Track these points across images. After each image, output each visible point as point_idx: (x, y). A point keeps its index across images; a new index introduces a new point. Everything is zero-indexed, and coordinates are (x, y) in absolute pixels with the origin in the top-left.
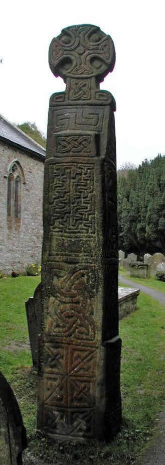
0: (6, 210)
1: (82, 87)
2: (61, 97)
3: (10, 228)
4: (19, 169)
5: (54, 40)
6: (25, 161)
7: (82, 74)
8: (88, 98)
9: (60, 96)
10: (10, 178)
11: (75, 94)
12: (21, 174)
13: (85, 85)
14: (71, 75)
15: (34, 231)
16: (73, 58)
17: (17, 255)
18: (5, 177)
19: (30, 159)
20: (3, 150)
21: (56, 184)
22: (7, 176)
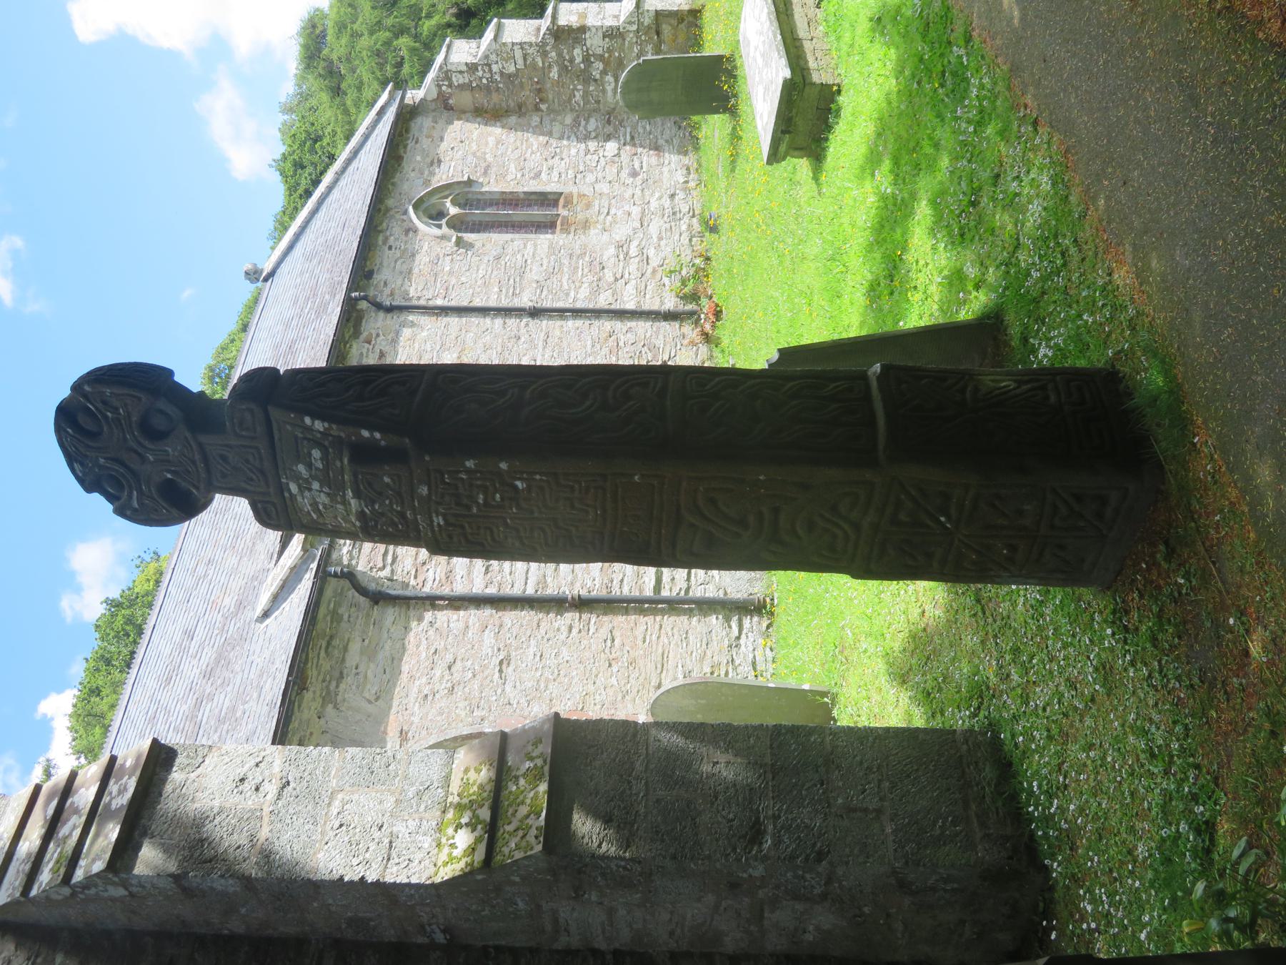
0: (542, 236)
2: (265, 510)
3: (586, 225)
4: (434, 200)
5: (120, 511)
6: (413, 185)
7: (194, 462)
10: (458, 224)
11: (252, 480)
12: (447, 193)
13: (224, 458)
14: (202, 486)
15: (592, 150)
17: (654, 204)
18: (459, 242)
19: (404, 164)
20: (390, 248)
22: (454, 239)
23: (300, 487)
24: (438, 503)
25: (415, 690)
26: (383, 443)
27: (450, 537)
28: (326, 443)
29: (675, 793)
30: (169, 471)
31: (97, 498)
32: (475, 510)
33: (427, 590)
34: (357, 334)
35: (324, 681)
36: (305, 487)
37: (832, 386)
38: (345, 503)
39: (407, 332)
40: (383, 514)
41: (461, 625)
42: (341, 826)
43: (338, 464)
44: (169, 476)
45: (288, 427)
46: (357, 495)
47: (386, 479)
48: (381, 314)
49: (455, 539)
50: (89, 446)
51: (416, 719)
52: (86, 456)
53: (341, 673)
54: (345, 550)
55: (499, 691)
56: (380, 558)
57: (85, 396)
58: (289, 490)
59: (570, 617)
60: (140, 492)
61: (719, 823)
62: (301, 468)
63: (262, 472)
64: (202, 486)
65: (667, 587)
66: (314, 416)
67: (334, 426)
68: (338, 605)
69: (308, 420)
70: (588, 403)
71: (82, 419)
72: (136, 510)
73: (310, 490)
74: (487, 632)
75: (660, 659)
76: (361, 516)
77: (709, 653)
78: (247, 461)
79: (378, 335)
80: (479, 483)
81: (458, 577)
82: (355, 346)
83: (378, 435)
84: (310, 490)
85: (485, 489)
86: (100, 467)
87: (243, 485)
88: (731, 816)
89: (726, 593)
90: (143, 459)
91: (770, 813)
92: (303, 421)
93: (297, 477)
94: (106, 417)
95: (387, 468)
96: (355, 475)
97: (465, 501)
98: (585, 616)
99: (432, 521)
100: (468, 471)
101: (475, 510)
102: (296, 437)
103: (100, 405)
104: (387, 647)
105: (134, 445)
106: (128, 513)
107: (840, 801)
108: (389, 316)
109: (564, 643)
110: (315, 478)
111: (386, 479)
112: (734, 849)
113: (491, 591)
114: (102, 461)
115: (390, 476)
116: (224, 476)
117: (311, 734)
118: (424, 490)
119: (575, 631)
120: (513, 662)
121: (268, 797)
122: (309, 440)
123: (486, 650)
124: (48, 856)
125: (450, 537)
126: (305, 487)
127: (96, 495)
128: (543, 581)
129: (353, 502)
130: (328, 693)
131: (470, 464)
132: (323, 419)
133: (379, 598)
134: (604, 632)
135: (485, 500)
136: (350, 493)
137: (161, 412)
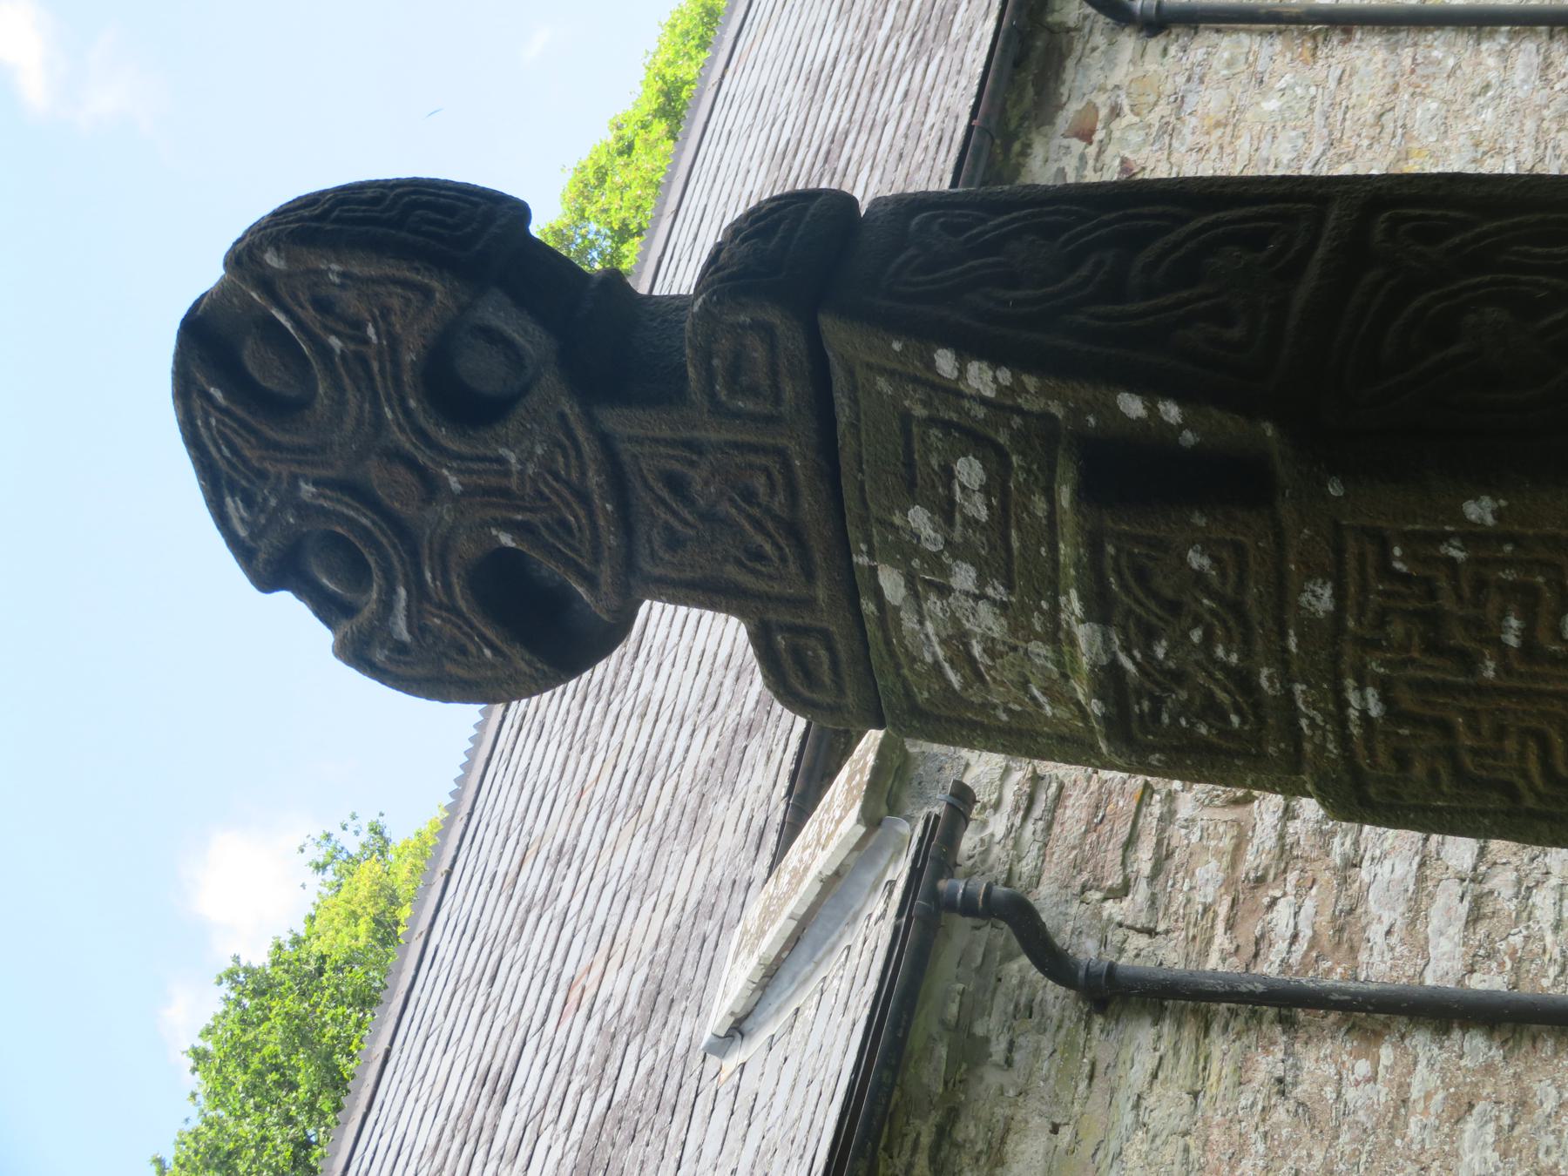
1: (688, 501)
2: (797, 653)
7: (584, 498)
8: (775, 470)
9: (787, 662)
11: (760, 556)
13: (676, 484)
14: (605, 573)
16: (466, 549)
21: (1525, 775)
23: (911, 580)
24: (1367, 644)
26: (1188, 438)
27: (1402, 759)
28: (1003, 438)
30: (508, 525)
31: (288, 606)
32: (1489, 671)
33: (1269, 968)
34: (1044, 106)
36: (928, 581)
38: (1057, 636)
39: (1210, 101)
40: (1178, 677)
41: (1382, 1094)
43: (1040, 506)
44: (506, 540)
45: (882, 384)
46: (1099, 609)
47: (1197, 560)
48: (1129, 42)
49: (1419, 769)
50: (277, 446)
52: (262, 475)
54: (998, 825)
56: (1113, 855)
57: (266, 284)
58: (878, 594)
60: (419, 592)
62: (919, 518)
63: (794, 531)
64: (605, 573)
66: (967, 349)
67: (1031, 382)
68: (974, 1006)
69: (945, 362)
71: (254, 358)
72: (401, 648)
73: (944, 591)
74: (1470, 1125)
76: (1109, 679)
78: (749, 496)
79: (1116, 112)
80: (1509, 575)
81: (1376, 932)
82: (1038, 150)
83: (1171, 412)
84: (944, 591)
85: (1526, 600)
86: (303, 509)
87: (732, 572)
90: (431, 487)
92: (930, 365)
93: (904, 551)
94: (325, 352)
95: (1199, 520)
96: (1094, 543)
97: (1458, 637)
99: (1343, 704)
100: (1473, 536)
101: (1489, 671)
102: (906, 417)
103: (309, 315)
105: (405, 442)
106: (379, 656)
108: (1155, 45)
110: (959, 551)
111: (1197, 560)
113: (1490, 982)
114: (307, 490)
115: (1207, 547)
116: (674, 542)
118: (1320, 599)
122: (947, 426)
125: (1402, 759)
126: (928, 581)
127: (285, 601)
129: (1082, 632)
131: (1480, 510)
132: (995, 360)
133: (1114, 995)
135: (1527, 635)
136: (1073, 603)
137: (491, 335)
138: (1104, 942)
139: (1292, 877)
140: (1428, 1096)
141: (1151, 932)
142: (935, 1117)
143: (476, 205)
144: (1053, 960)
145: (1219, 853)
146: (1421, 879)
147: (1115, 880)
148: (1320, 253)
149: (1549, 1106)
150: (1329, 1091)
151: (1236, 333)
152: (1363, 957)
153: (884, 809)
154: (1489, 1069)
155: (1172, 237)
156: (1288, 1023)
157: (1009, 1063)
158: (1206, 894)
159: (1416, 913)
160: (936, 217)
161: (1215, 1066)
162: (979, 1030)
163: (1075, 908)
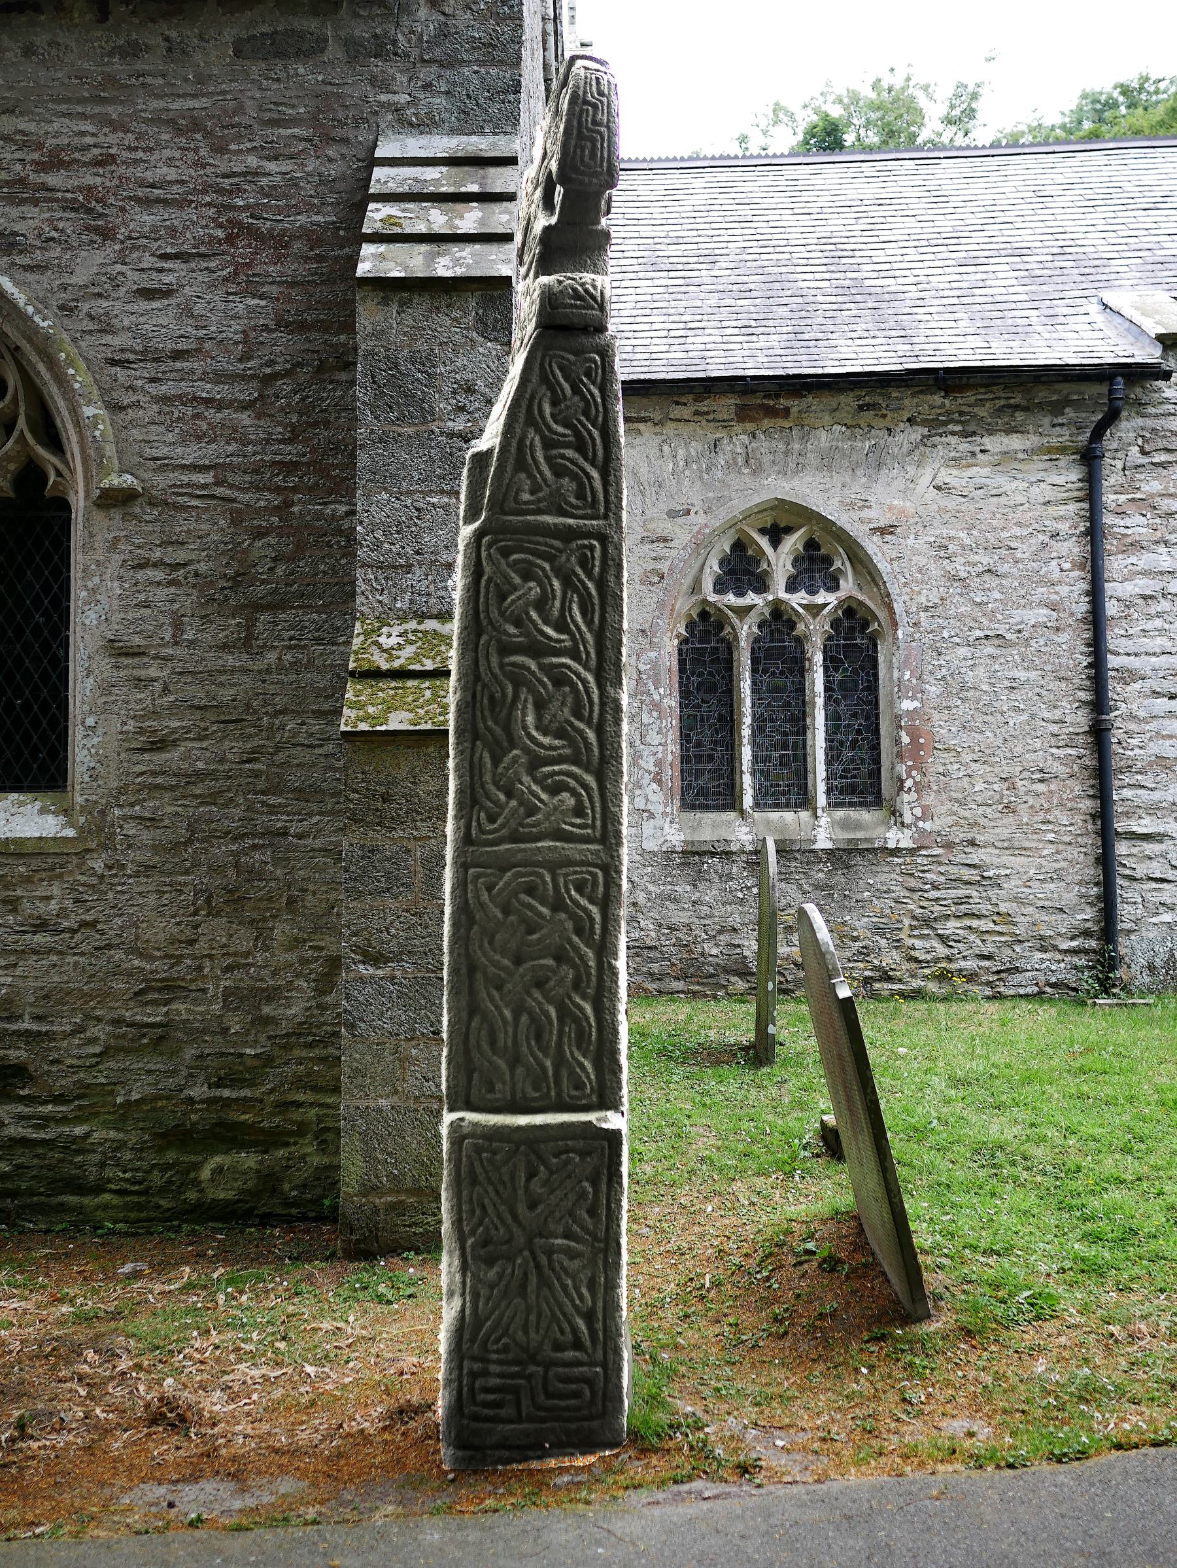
25: (953, 533)
29: (419, 869)
33: (1108, 519)
35: (961, 413)
37: (587, 1064)
41: (1056, 575)
42: (418, 509)
51: (911, 541)
53: (974, 434)
55: (957, 640)
59: (1081, 720)
61: (385, 918)
65: (1135, 851)
68: (1078, 405)
70: (546, 741)
74: (1046, 611)
75: (1016, 844)
77: (1030, 910)
81: (1133, 559)
88: (393, 931)
89: (1130, 932)
91: (398, 974)
98: (1080, 740)
104: (1015, 484)
107: (414, 1052)
109: (1033, 716)
112: (355, 934)
113: (1111, 608)
117: (884, 416)
119: (1055, 728)
120: (1003, 651)
121: (450, 424)
123: (1018, 615)
124: (411, 206)
128: (1131, 676)
130: (945, 423)
133: (1090, 459)
134: (1057, 768)
138: (1116, 450)
139: (1158, 521)
140: (1057, 593)
141: (1124, 469)
142: (1024, 403)
143: (601, 166)
144: (1098, 433)
145: (1166, 488)
146: (1161, 573)
147: (1147, 448)
148: (571, 521)
149: (1058, 640)
150: (1054, 555)
151: (526, 497)
152: (1120, 556)
153: (1169, 343)
154: (1072, 614)
155: (581, 461)
156: (1084, 534)
157: (1054, 426)
158: (1145, 487)
159: (1145, 573)
160: (595, 362)
161: (1063, 507)
162: (1067, 410)
163: (1132, 435)
